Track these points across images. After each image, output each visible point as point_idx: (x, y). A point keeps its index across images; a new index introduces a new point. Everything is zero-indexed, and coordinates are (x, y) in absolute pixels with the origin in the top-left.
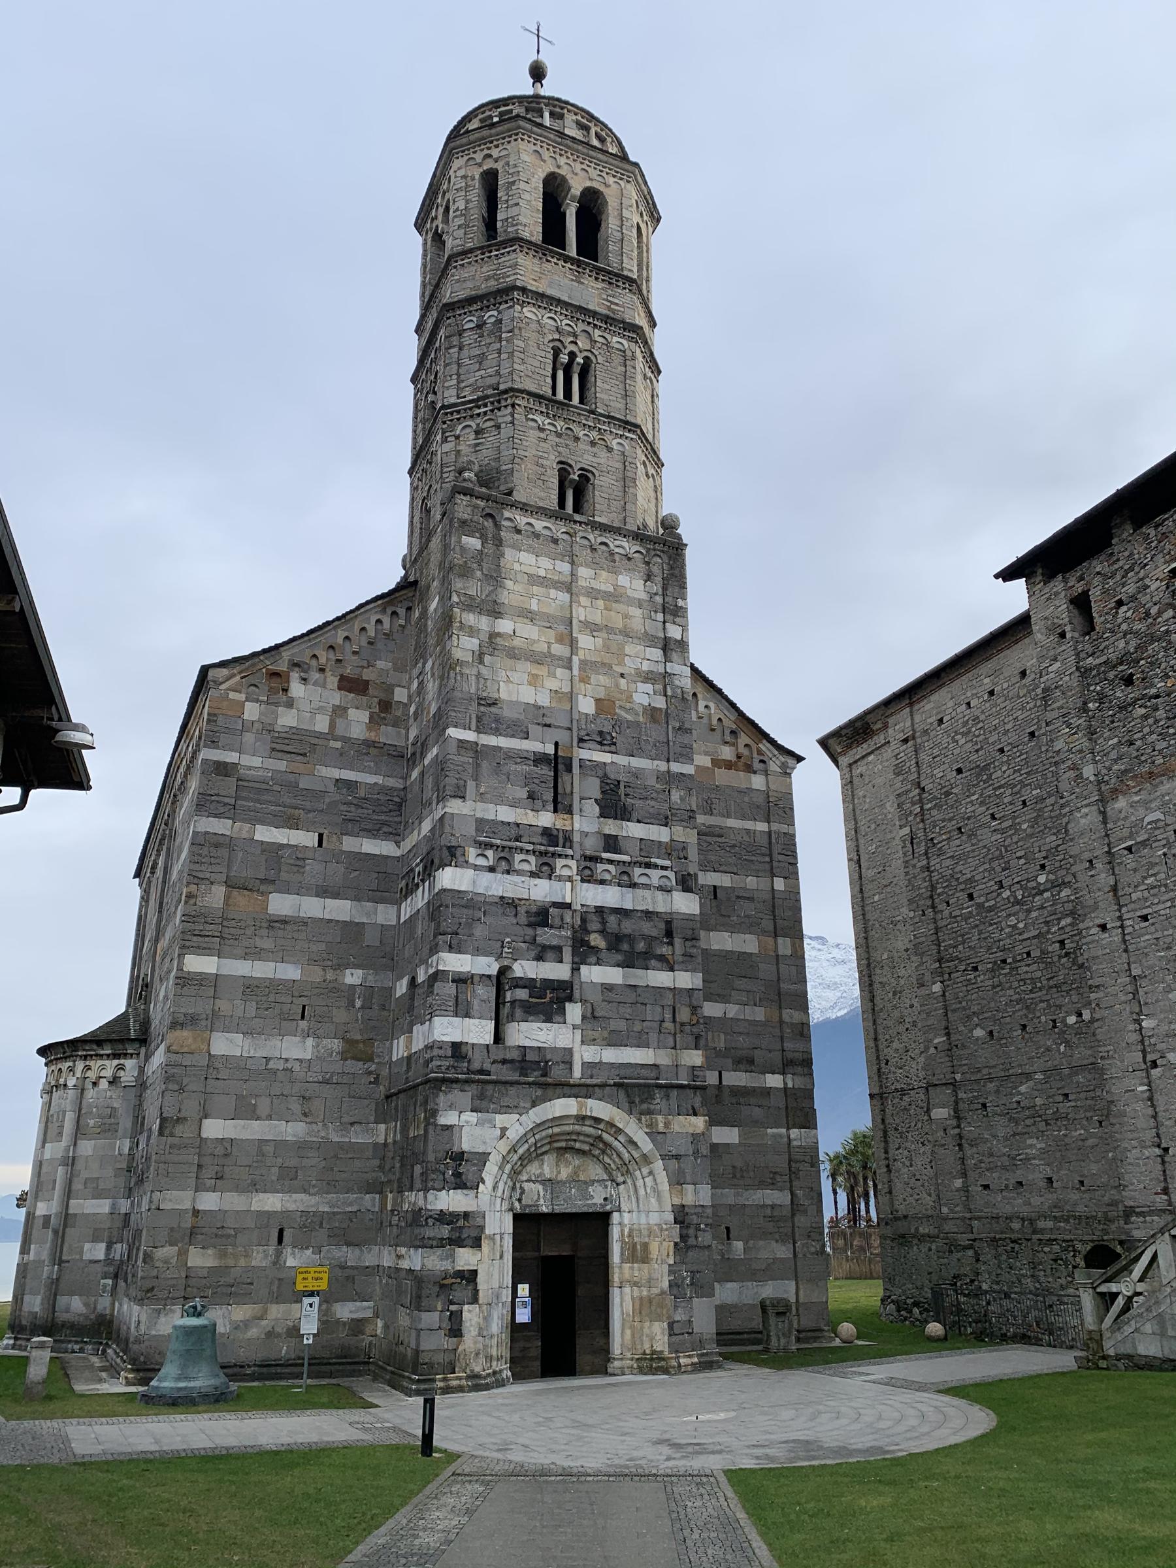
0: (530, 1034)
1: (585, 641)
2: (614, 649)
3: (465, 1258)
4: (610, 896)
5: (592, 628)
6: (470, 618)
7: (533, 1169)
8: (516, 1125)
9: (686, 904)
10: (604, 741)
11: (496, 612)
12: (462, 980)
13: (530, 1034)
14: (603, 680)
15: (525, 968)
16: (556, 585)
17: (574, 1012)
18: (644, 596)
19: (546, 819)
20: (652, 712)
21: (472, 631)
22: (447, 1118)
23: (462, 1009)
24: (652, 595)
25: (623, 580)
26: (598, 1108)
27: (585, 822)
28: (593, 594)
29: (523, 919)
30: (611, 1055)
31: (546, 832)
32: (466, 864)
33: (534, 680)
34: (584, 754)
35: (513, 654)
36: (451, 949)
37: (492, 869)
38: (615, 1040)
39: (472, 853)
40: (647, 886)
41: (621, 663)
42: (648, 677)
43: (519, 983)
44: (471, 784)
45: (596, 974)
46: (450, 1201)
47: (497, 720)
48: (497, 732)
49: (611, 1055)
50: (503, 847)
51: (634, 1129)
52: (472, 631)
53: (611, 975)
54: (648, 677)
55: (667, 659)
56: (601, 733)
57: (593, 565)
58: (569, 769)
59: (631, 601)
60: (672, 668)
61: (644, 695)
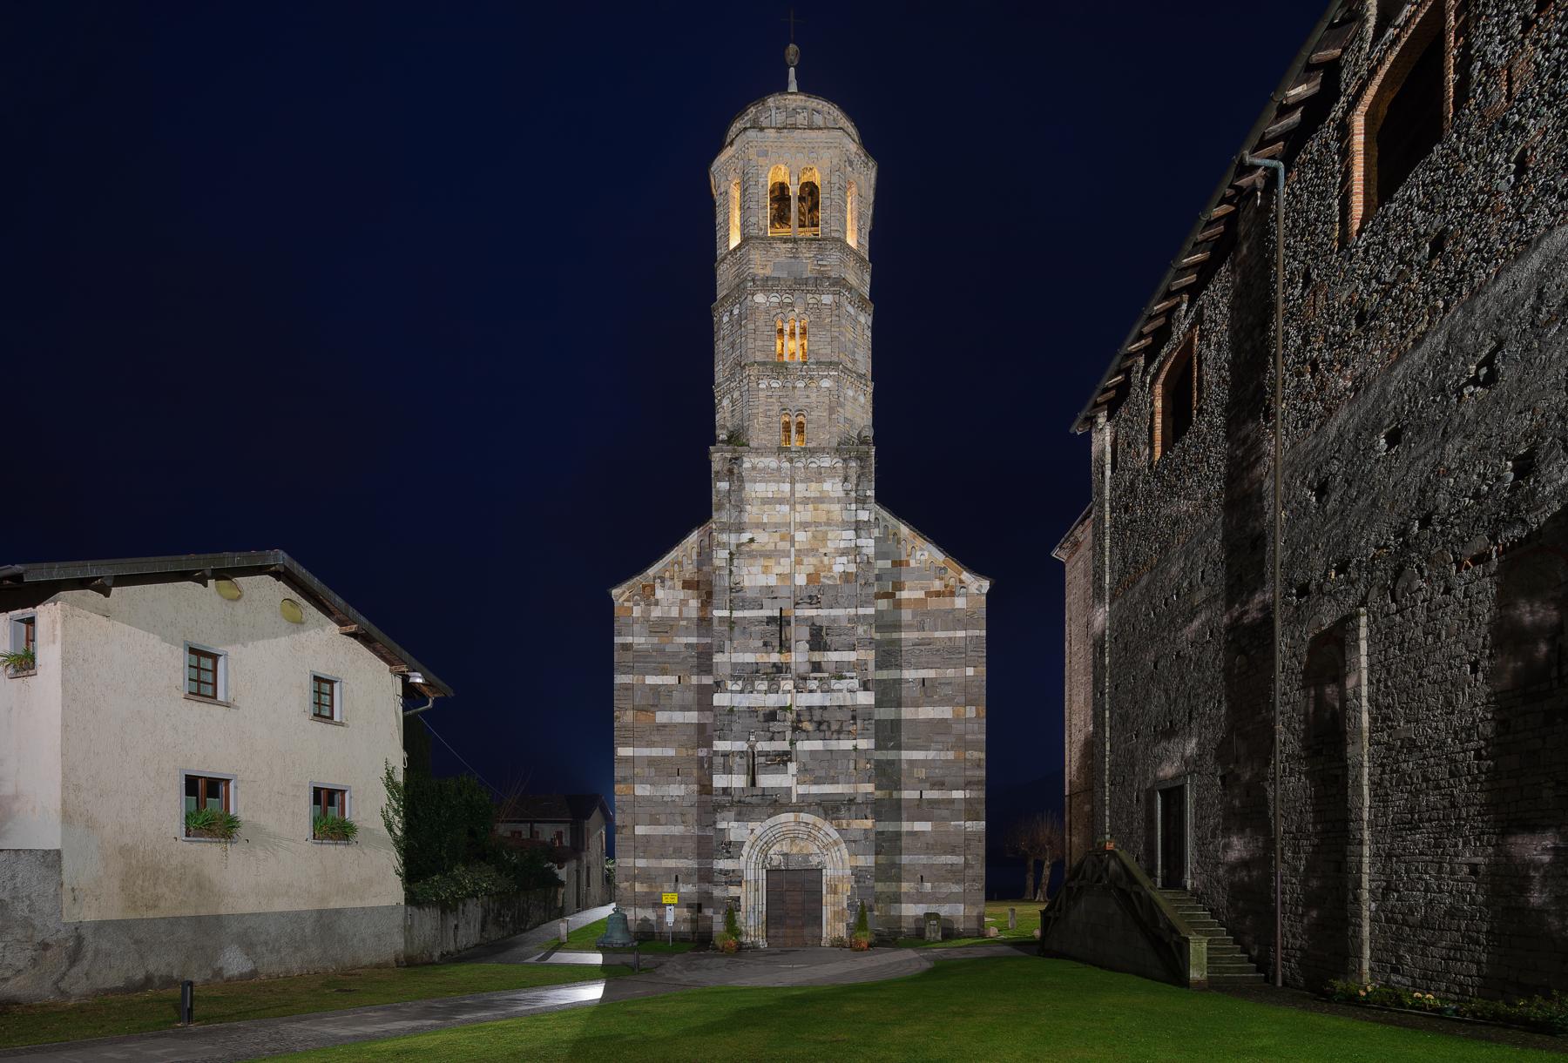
0: (767, 781)
1: (800, 536)
2: (820, 535)
3: (734, 891)
4: (817, 699)
5: (804, 526)
6: (724, 537)
7: (776, 848)
8: (758, 827)
9: (866, 699)
10: (813, 601)
11: (740, 528)
12: (726, 755)
13: (767, 781)
14: (813, 560)
15: (763, 746)
16: (781, 501)
17: (792, 767)
18: (842, 494)
19: (775, 657)
20: (846, 576)
21: (724, 545)
22: (722, 825)
23: (728, 770)
24: (847, 493)
25: (827, 486)
26: (804, 817)
27: (799, 656)
28: (806, 501)
29: (761, 718)
30: (815, 789)
31: (774, 665)
32: (726, 691)
33: (766, 570)
34: (799, 612)
35: (752, 555)
36: (720, 739)
37: (742, 692)
38: (816, 782)
39: (730, 685)
40: (840, 690)
41: (825, 546)
42: (844, 553)
43: (761, 754)
44: (727, 643)
45: (805, 746)
46: (722, 864)
47: (743, 600)
48: (743, 608)
49: (815, 789)
50: (748, 676)
51: (829, 829)
52: (724, 545)
53: (817, 745)
54: (844, 553)
55: (858, 537)
56: (810, 597)
57: (807, 480)
58: (789, 624)
59: (831, 500)
60: (860, 542)
61: (840, 565)
